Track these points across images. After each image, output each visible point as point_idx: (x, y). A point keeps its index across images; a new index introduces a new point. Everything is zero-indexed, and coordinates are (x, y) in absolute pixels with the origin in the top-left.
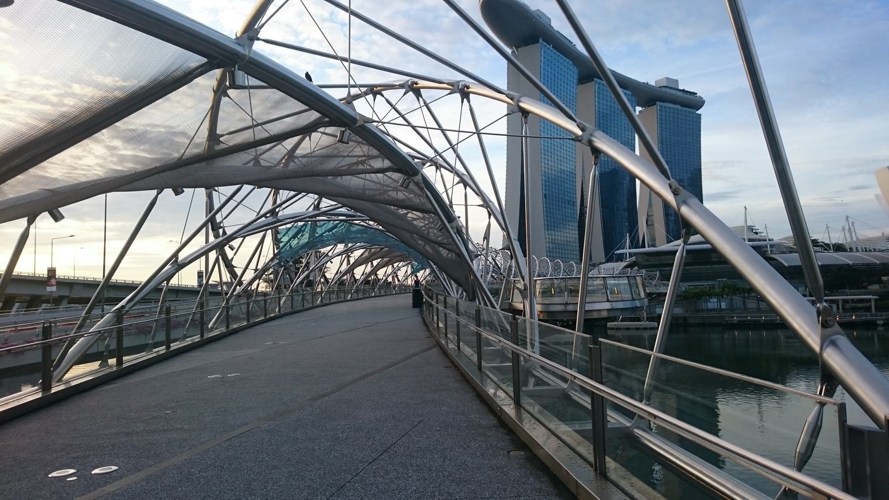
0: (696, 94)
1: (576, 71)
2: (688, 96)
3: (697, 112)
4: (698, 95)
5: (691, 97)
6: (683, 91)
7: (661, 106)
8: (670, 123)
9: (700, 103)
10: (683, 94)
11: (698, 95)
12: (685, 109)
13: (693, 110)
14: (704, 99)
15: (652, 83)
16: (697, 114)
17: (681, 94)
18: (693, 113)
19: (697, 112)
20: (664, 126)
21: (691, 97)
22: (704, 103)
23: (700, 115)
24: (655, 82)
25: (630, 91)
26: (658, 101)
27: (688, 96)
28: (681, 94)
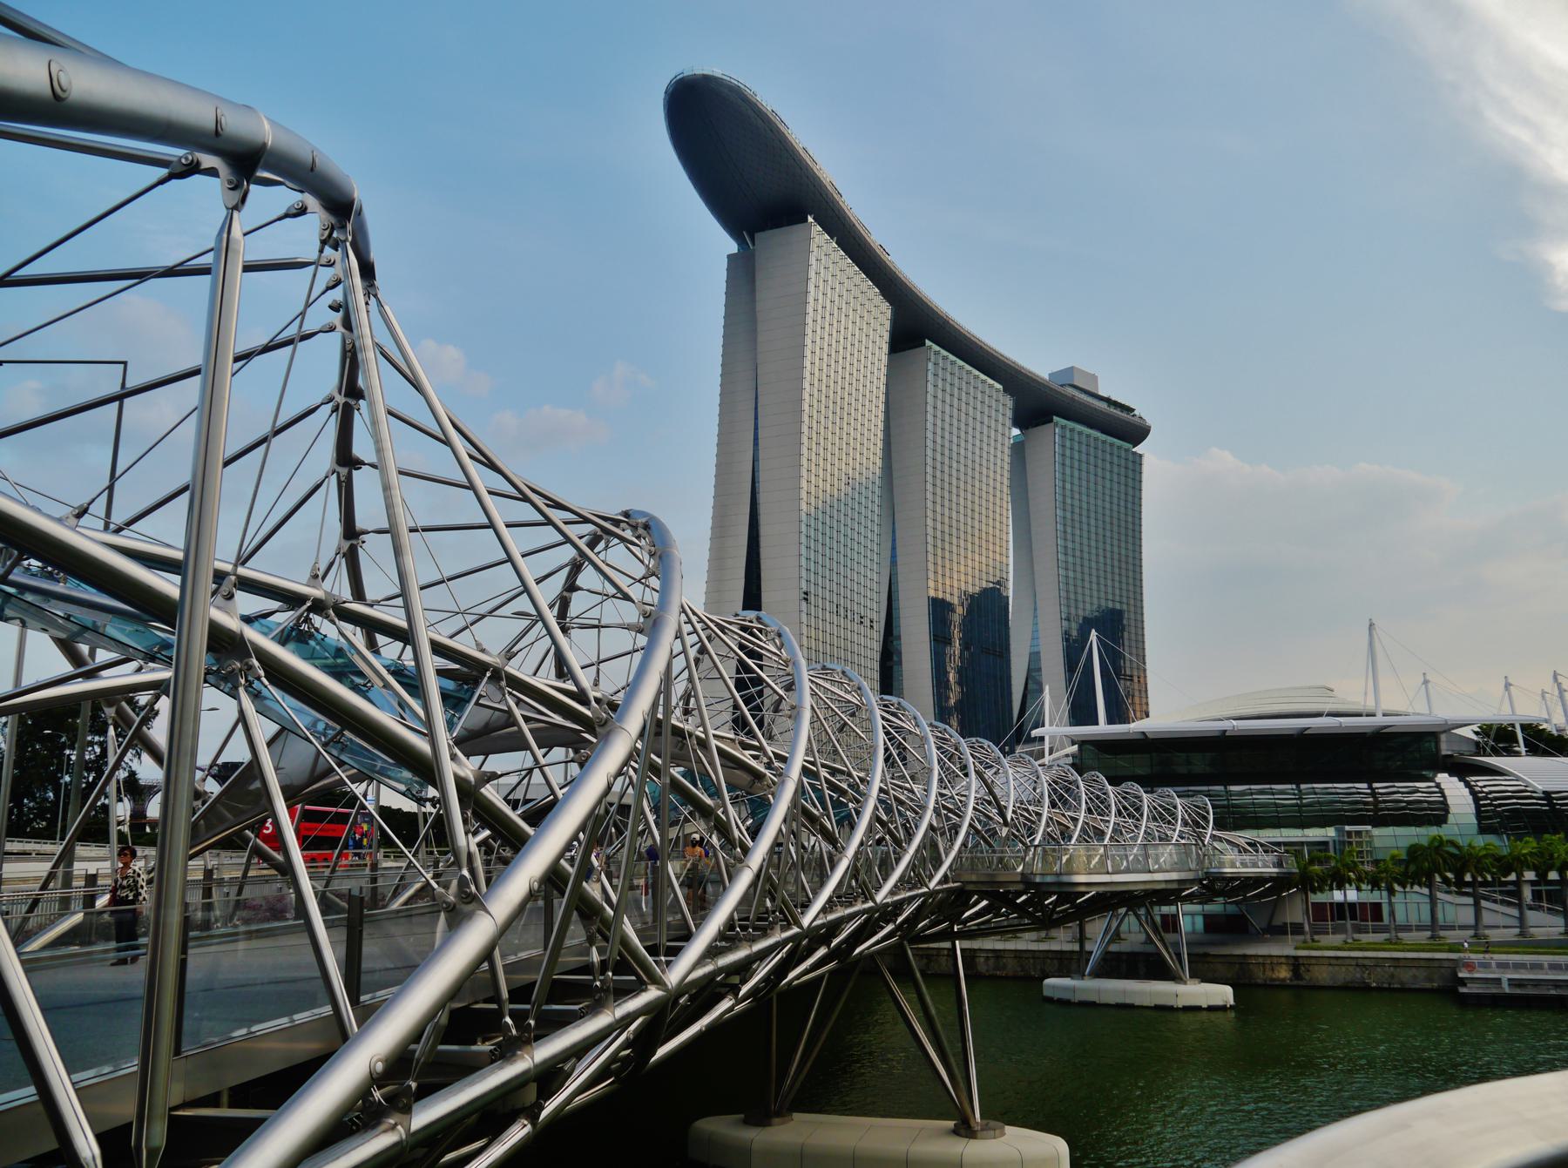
0: (1133, 410)
1: (889, 313)
2: (1117, 412)
3: (1134, 450)
4: (1136, 412)
5: (1124, 415)
6: (1108, 400)
7: (1063, 427)
8: (1079, 465)
9: (1138, 433)
10: (1109, 406)
11: (1136, 412)
12: (1110, 439)
13: (1127, 445)
14: (1149, 422)
15: (1046, 377)
16: (1135, 453)
17: (1103, 406)
18: (1127, 450)
19: (1134, 450)
20: (1068, 471)
21: (1124, 415)
22: (1149, 431)
23: (1141, 456)
24: (1050, 374)
25: (1000, 383)
26: (1058, 416)
27: (1117, 412)
28: (1103, 406)
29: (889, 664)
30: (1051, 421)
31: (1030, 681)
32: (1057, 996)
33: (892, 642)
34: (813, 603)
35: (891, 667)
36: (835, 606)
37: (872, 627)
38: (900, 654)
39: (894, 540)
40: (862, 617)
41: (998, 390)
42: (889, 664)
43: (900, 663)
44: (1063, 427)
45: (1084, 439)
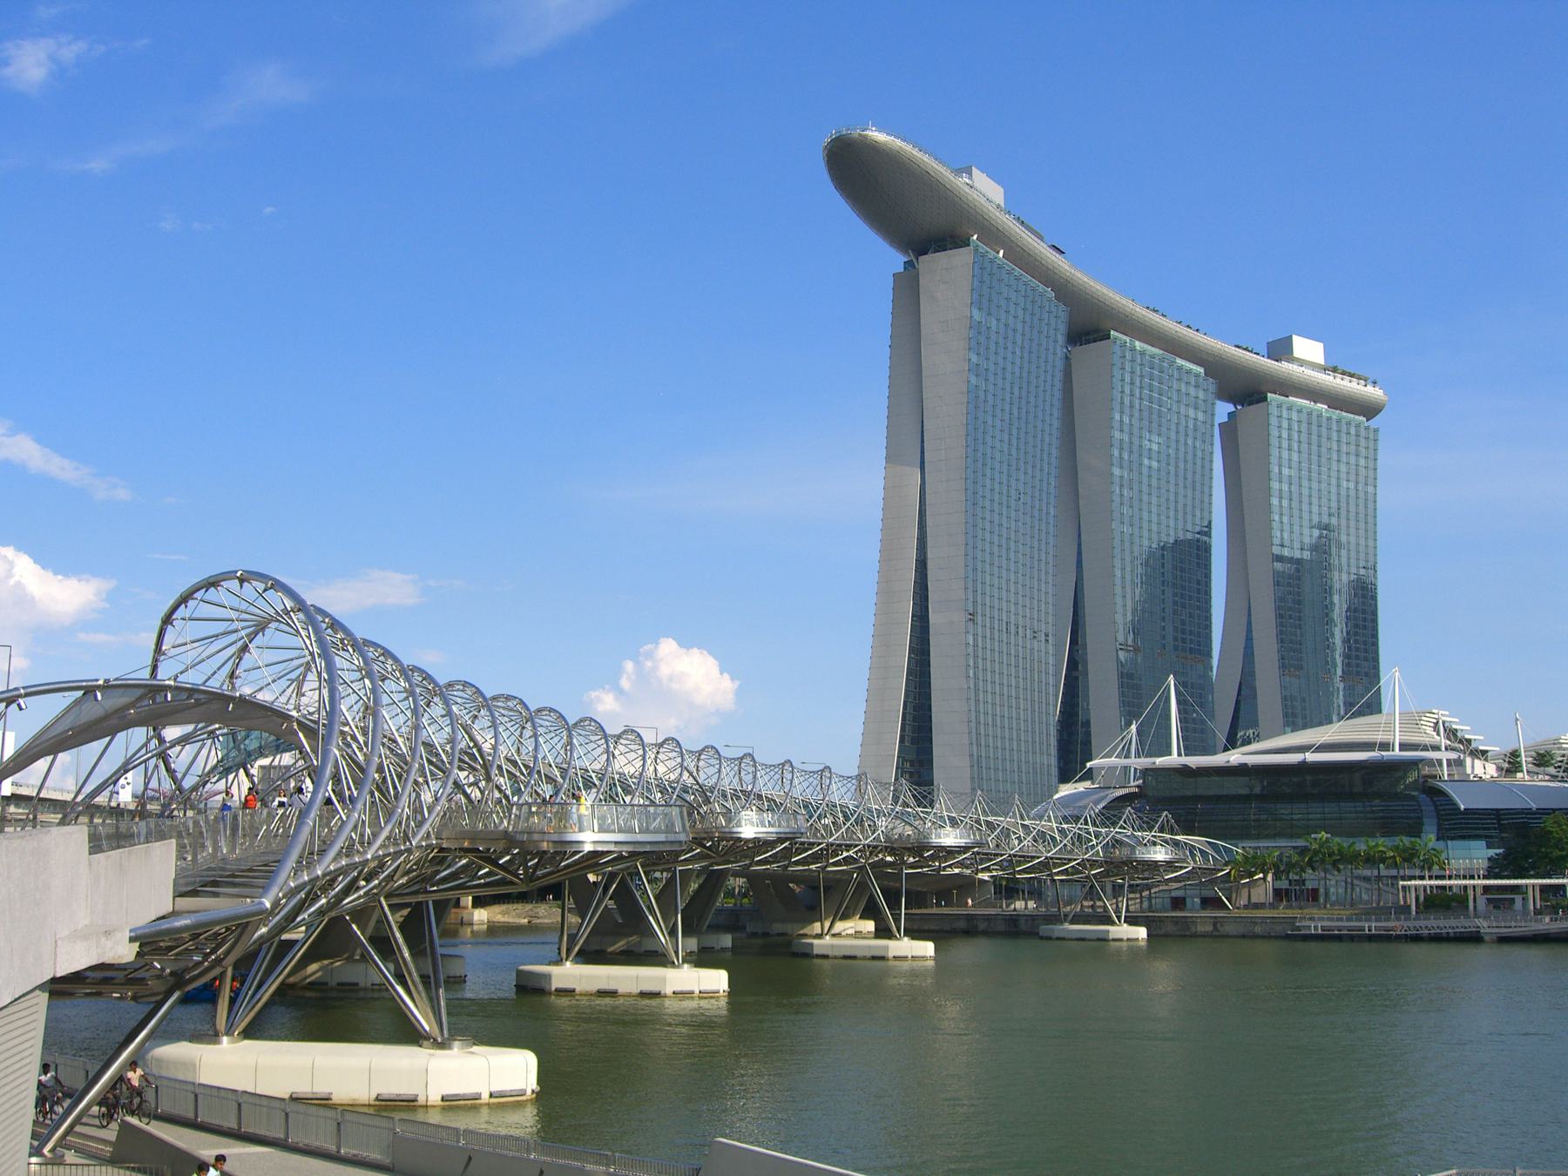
12: (1335, 414)
29: (1075, 674)
30: (1265, 399)
31: (1243, 687)
32: (1045, 935)
33: (1078, 651)
34: (980, 622)
35: (1076, 678)
36: (1005, 624)
37: (1047, 641)
38: (1086, 663)
39: (1080, 545)
40: (1034, 632)
41: (1197, 375)
42: (1075, 674)
43: (1086, 673)
44: (1279, 406)
45: (1304, 417)
